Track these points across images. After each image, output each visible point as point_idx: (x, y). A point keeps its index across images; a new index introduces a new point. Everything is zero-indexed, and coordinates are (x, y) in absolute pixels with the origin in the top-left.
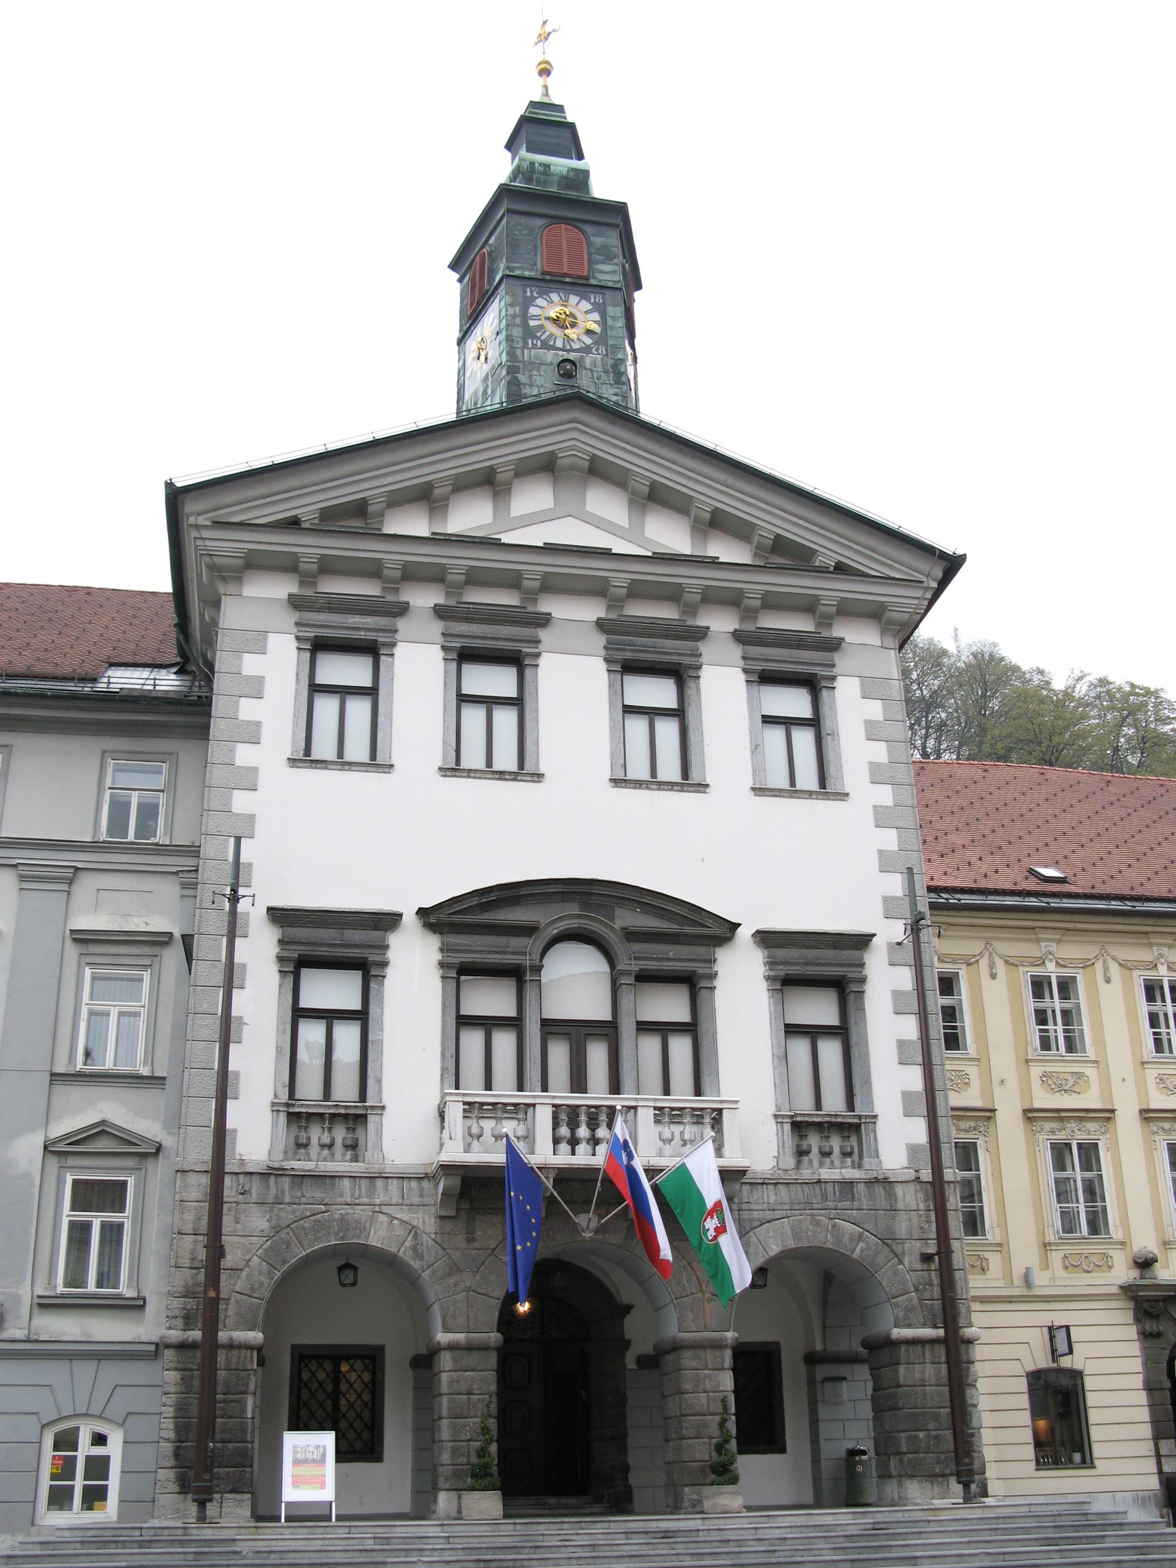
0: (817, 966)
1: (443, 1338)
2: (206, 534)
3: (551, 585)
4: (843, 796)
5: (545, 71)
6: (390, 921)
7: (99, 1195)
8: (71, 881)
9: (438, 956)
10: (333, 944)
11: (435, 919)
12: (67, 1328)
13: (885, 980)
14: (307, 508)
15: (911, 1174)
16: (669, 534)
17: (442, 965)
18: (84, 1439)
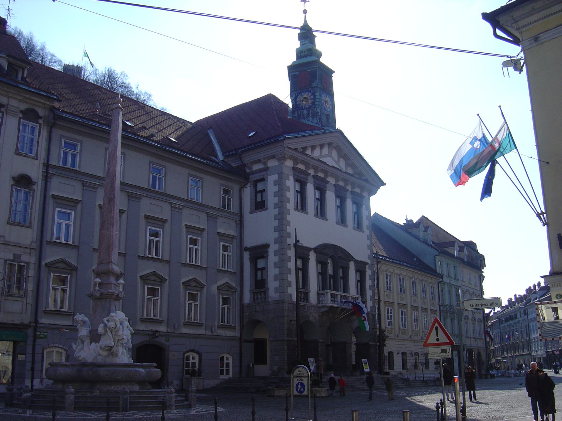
0: (361, 268)
1: (320, 340)
2: (286, 149)
3: (333, 175)
4: (363, 232)
5: (305, 12)
6: (309, 249)
7: (225, 301)
8: (217, 219)
9: (315, 259)
10: (302, 253)
11: (316, 250)
12: (222, 332)
13: (368, 272)
14: (299, 146)
15: (371, 313)
16: (342, 165)
17: (316, 261)
18: (225, 359)
